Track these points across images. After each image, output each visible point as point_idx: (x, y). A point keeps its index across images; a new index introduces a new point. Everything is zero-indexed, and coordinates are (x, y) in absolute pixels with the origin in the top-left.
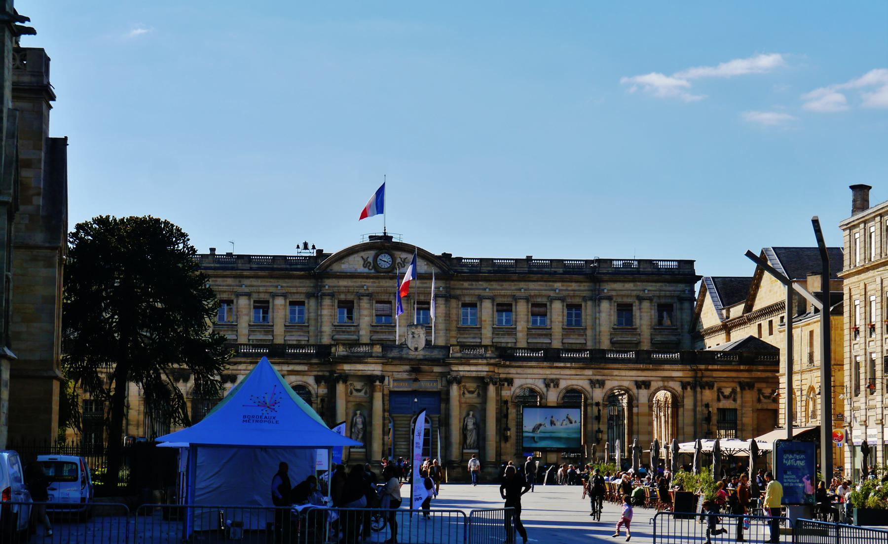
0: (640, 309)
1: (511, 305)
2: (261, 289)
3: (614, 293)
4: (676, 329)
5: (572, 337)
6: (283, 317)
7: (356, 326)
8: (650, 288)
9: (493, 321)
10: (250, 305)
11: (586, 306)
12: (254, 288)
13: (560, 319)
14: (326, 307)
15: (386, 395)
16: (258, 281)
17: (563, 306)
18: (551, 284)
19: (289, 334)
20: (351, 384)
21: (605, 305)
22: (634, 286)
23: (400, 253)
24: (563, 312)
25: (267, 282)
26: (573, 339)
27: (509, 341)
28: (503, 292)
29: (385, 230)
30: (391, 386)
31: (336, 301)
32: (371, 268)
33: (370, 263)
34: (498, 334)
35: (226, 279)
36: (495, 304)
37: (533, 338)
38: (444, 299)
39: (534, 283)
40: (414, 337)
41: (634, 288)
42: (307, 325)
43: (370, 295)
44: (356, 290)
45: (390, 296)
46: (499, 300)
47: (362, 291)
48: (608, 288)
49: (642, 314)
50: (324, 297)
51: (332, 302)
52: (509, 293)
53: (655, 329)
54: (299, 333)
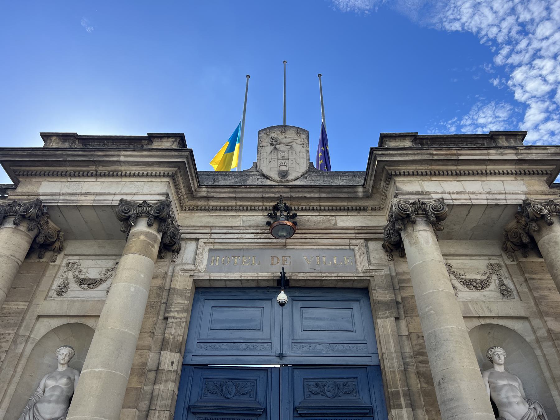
15: (181, 293)
20: (71, 266)
30: (203, 265)
40: (276, 149)
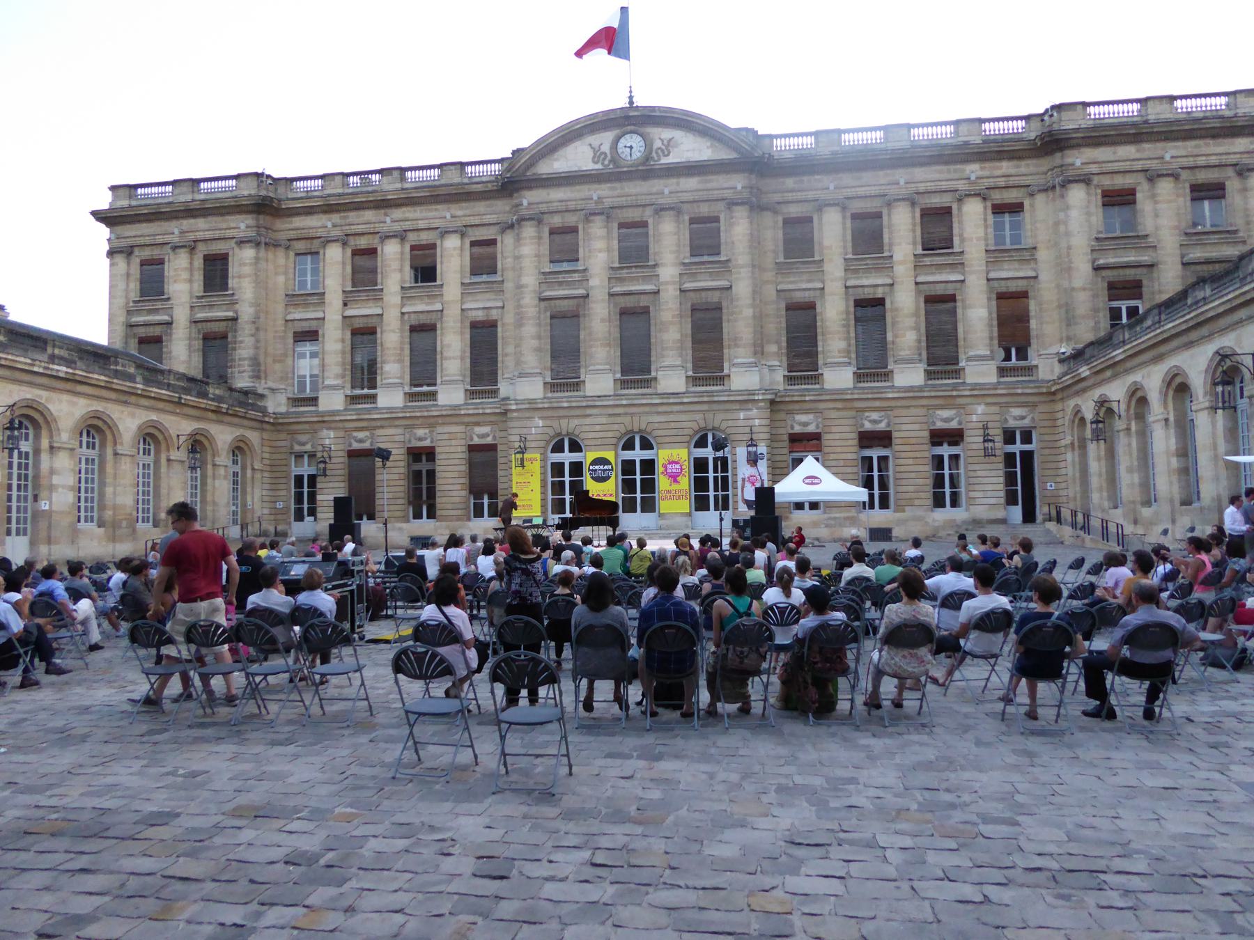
0: (1153, 197)
1: (879, 216)
2: (421, 224)
3: (1094, 168)
4: (1236, 232)
5: (1006, 266)
6: (459, 269)
7: (585, 270)
8: (1174, 153)
9: (845, 247)
10: (402, 253)
11: (1032, 206)
12: (409, 223)
13: (981, 232)
14: (528, 241)
16: (415, 211)
17: (985, 208)
18: (958, 166)
19: (470, 299)
21: (1077, 194)
22: (1138, 151)
23: (660, 129)
24: (985, 220)
25: (430, 211)
26: (1009, 270)
27: (880, 281)
28: (861, 191)
29: (631, 92)
31: (546, 230)
32: (606, 162)
33: (605, 154)
34: (856, 271)
35: (362, 213)
36: (848, 215)
37: (926, 274)
38: (747, 207)
39: (923, 169)
41: (1138, 156)
42: (500, 279)
43: (607, 213)
44: (581, 204)
45: (644, 211)
46: (858, 206)
47: (591, 206)
48: (1078, 159)
49: (1159, 206)
50: (523, 223)
51: (539, 232)
52: (873, 190)
53: (1186, 234)
54: (487, 296)
